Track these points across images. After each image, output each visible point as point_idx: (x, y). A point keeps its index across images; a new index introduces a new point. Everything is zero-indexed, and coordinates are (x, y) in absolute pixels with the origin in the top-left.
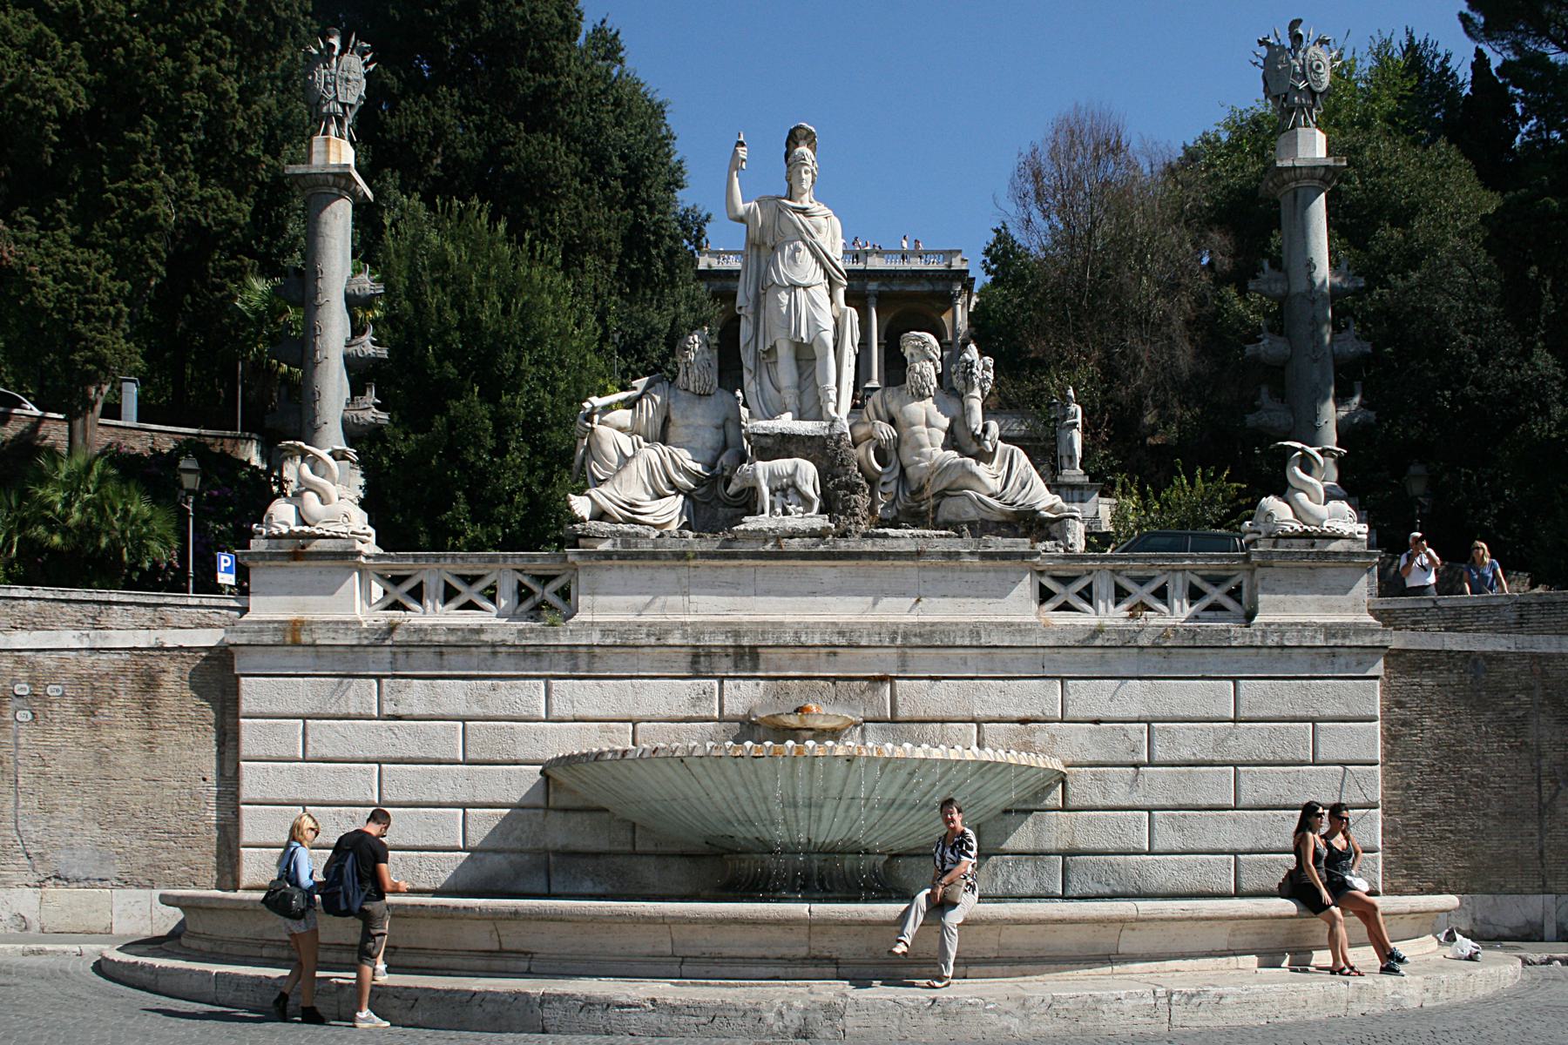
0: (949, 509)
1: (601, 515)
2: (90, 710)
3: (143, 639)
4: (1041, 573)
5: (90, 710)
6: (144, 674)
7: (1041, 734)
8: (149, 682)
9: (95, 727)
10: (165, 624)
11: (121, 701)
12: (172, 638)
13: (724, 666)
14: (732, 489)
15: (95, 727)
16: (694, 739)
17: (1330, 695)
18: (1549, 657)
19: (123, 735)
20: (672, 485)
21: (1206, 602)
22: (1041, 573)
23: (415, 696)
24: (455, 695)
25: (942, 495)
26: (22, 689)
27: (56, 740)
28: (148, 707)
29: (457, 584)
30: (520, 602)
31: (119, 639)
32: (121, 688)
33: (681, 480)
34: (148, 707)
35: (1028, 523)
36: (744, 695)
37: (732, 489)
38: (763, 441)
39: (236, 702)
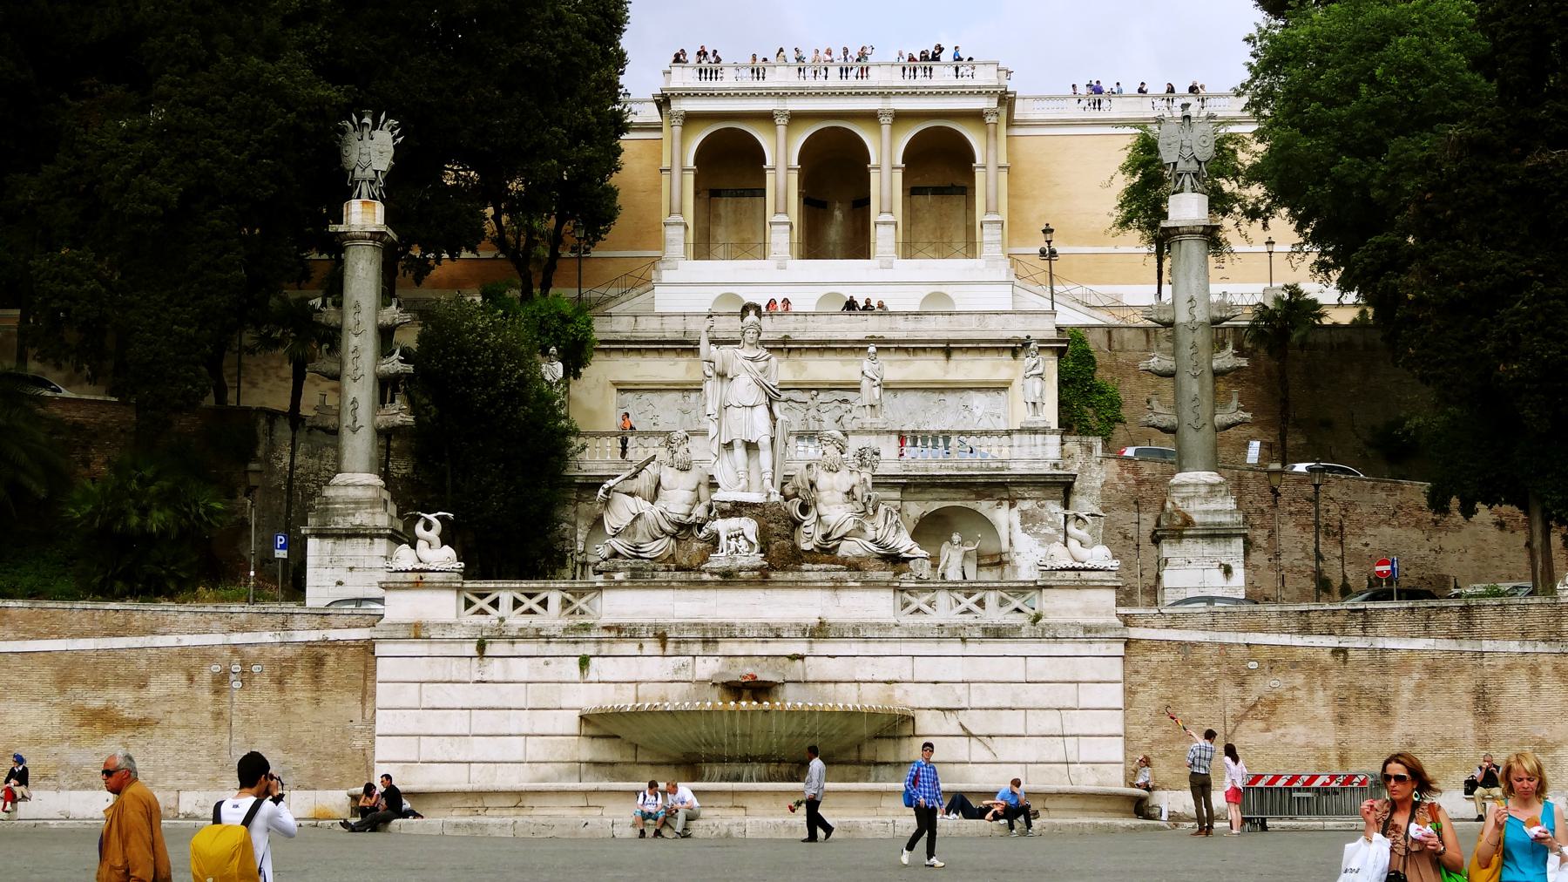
0: (848, 549)
1: (616, 554)
2: (280, 682)
3: (314, 636)
4: (902, 590)
5: (280, 682)
6: (316, 657)
7: (898, 691)
8: (318, 662)
9: (281, 690)
10: (329, 626)
11: (299, 674)
12: (333, 635)
13: (697, 648)
14: (702, 535)
15: (281, 690)
16: (676, 698)
17: (1086, 669)
18: (1231, 645)
19: (300, 695)
20: (663, 532)
21: (1012, 607)
22: (902, 590)
23: (495, 669)
24: (521, 669)
25: (841, 538)
26: (237, 668)
27: (256, 699)
28: (316, 679)
29: (522, 598)
30: (564, 608)
31: (300, 636)
32: (299, 665)
33: (668, 528)
34: (316, 679)
35: (894, 560)
36: (708, 667)
37: (702, 535)
38: (724, 506)
39: (374, 673)
